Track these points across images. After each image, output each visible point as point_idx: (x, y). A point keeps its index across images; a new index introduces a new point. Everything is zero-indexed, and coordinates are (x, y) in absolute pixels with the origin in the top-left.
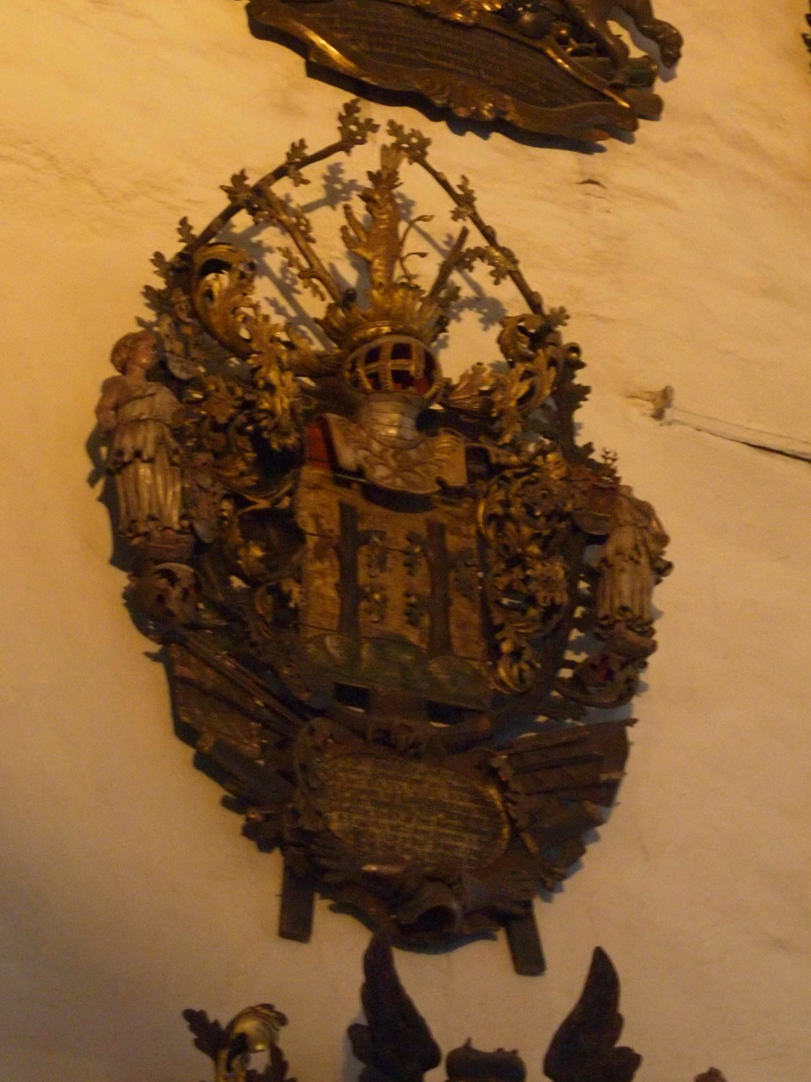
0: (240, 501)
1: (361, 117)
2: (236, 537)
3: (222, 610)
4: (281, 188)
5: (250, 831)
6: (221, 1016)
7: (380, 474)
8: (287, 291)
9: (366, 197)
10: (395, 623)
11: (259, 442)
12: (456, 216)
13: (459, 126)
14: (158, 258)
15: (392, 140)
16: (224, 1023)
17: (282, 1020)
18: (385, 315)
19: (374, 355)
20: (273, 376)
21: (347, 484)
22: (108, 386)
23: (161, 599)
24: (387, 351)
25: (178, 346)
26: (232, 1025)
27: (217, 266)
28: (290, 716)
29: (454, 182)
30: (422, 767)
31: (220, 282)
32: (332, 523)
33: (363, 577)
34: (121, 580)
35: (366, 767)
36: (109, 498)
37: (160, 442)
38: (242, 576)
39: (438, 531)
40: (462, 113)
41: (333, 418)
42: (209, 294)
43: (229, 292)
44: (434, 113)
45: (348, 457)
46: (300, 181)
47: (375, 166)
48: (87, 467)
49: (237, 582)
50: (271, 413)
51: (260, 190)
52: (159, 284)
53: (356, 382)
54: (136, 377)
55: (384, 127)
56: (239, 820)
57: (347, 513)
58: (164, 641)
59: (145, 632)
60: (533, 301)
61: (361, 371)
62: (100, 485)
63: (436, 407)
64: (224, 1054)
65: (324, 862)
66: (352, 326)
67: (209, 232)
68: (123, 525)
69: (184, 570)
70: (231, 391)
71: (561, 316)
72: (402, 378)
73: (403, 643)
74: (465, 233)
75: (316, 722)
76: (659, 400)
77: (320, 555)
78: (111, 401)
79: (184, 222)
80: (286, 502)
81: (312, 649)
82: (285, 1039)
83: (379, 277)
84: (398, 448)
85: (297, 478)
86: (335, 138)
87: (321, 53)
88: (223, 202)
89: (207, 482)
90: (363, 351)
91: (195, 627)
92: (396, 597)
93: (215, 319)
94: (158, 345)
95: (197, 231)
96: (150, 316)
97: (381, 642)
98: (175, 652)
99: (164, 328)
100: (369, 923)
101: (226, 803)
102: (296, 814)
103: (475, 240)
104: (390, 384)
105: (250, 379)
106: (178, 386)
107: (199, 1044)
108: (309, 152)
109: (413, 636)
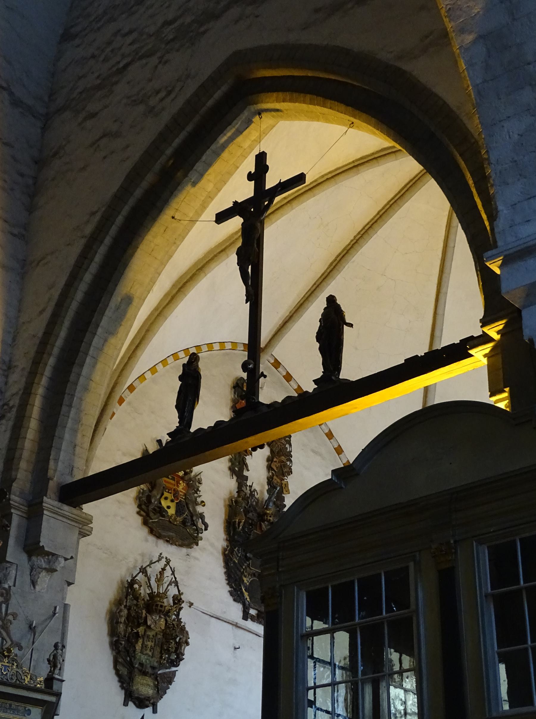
1: (162, 556)
2: (131, 637)
19: (157, 605)
29: (173, 568)
46: (151, 567)
55: (165, 558)
57: (145, 631)
60: (179, 591)
71: (182, 594)
74: (172, 578)
76: (191, 604)
86: (157, 559)
97: (146, 654)
103: (174, 579)
108: (153, 562)
109: (150, 654)
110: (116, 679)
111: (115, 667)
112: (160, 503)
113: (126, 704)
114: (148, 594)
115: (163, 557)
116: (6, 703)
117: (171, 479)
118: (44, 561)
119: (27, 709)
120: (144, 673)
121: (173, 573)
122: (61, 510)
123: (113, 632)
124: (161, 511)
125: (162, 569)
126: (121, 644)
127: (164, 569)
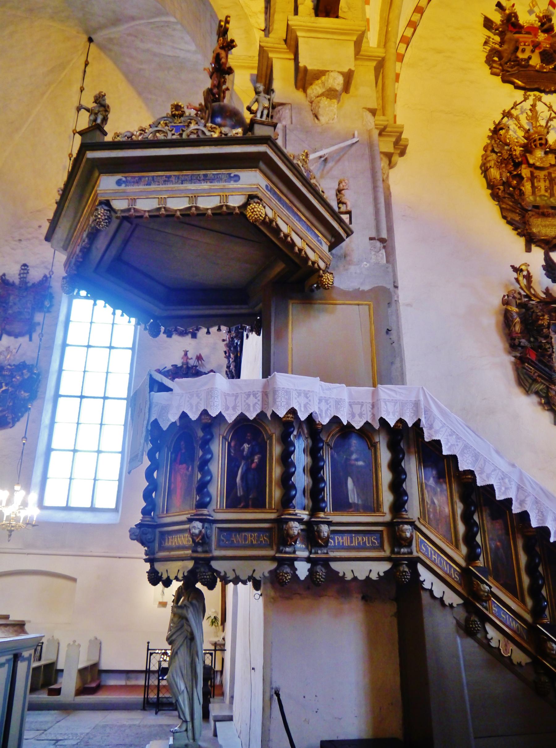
0: (510, 172)
2: (511, 179)
3: (509, 194)
4: (513, 111)
5: (519, 234)
6: (517, 266)
7: (538, 164)
8: (515, 132)
9: (530, 110)
10: (543, 192)
11: (514, 161)
12: (549, 111)
13: (547, 93)
14: (490, 129)
15: (534, 97)
16: (518, 267)
17: (529, 265)
18: (536, 132)
19: (535, 141)
20: (515, 148)
21: (531, 167)
22: (483, 156)
23: (498, 193)
24: (538, 139)
25: (496, 145)
26: (519, 267)
27: (502, 129)
28: (524, 212)
29: (548, 104)
30: (551, 218)
31: (502, 132)
32: (529, 175)
33: (536, 184)
34: (490, 191)
35: (540, 220)
36: (485, 177)
37: (495, 164)
38: (513, 188)
39: (550, 174)
40: (547, 90)
41: (528, 155)
42: (501, 135)
43: (505, 133)
44: (541, 91)
45: (531, 161)
46: (516, 109)
47: (532, 103)
48: (480, 171)
49: (511, 189)
50: (516, 155)
51: (509, 112)
52: (491, 134)
53: (531, 147)
54: (489, 152)
55: (532, 96)
56: (516, 232)
57: (532, 173)
58: (499, 201)
59: (494, 200)
61: (532, 144)
62: (483, 174)
63: (548, 150)
64: (519, 272)
65: (533, 238)
66: (529, 136)
67: (499, 123)
68: (489, 180)
69: (501, 187)
70: (507, 152)
72: (541, 144)
73: (545, 196)
74: (551, 114)
75: (529, 212)
77: (527, 181)
78: (484, 158)
79: (494, 121)
80: (520, 172)
81: (527, 199)
82: (530, 269)
83: (534, 125)
84: (541, 159)
85: (521, 167)
86: (523, 99)
87: (517, 83)
88: (502, 116)
89: (504, 170)
90: (532, 141)
91: (505, 198)
92: (543, 188)
93: (502, 139)
94: (492, 146)
95: (497, 123)
96: (489, 142)
97: (540, 196)
98: (501, 203)
99: (493, 142)
100: (543, 248)
101: (513, 229)
102: (527, 230)
104: (538, 145)
105: (510, 150)
106: (496, 153)
107: (514, 271)
108: (518, 103)
109: (547, 194)
110: (509, 228)
111: (504, 217)
112: (518, 57)
113: (528, 250)
114: (523, 137)
115: (530, 95)
116: (199, 175)
117: (525, 34)
118: (320, 87)
119: (232, 175)
120: (544, 215)
121: (550, 108)
122: (316, 23)
123: (491, 185)
124: (517, 62)
125: (532, 105)
126: (499, 189)
127: (534, 106)
